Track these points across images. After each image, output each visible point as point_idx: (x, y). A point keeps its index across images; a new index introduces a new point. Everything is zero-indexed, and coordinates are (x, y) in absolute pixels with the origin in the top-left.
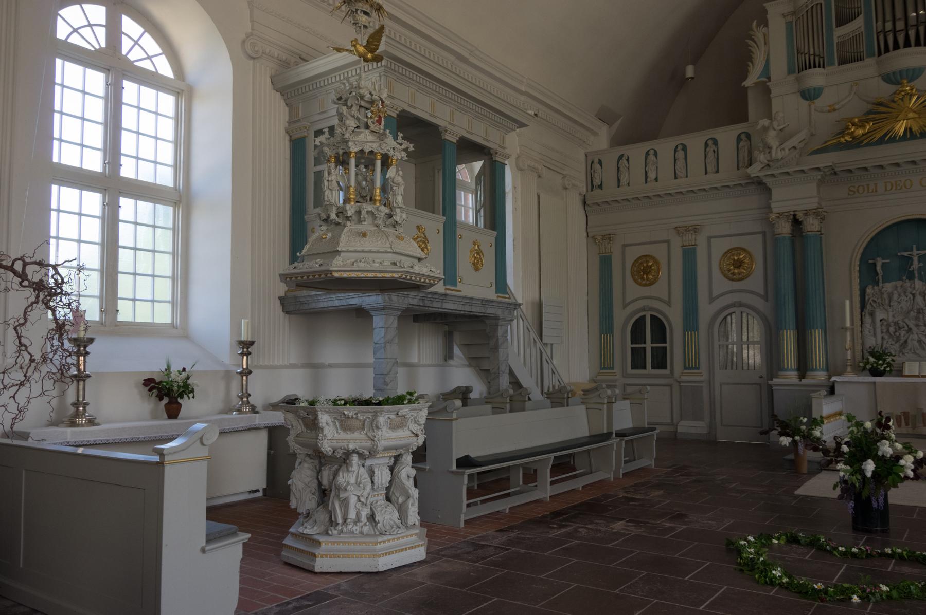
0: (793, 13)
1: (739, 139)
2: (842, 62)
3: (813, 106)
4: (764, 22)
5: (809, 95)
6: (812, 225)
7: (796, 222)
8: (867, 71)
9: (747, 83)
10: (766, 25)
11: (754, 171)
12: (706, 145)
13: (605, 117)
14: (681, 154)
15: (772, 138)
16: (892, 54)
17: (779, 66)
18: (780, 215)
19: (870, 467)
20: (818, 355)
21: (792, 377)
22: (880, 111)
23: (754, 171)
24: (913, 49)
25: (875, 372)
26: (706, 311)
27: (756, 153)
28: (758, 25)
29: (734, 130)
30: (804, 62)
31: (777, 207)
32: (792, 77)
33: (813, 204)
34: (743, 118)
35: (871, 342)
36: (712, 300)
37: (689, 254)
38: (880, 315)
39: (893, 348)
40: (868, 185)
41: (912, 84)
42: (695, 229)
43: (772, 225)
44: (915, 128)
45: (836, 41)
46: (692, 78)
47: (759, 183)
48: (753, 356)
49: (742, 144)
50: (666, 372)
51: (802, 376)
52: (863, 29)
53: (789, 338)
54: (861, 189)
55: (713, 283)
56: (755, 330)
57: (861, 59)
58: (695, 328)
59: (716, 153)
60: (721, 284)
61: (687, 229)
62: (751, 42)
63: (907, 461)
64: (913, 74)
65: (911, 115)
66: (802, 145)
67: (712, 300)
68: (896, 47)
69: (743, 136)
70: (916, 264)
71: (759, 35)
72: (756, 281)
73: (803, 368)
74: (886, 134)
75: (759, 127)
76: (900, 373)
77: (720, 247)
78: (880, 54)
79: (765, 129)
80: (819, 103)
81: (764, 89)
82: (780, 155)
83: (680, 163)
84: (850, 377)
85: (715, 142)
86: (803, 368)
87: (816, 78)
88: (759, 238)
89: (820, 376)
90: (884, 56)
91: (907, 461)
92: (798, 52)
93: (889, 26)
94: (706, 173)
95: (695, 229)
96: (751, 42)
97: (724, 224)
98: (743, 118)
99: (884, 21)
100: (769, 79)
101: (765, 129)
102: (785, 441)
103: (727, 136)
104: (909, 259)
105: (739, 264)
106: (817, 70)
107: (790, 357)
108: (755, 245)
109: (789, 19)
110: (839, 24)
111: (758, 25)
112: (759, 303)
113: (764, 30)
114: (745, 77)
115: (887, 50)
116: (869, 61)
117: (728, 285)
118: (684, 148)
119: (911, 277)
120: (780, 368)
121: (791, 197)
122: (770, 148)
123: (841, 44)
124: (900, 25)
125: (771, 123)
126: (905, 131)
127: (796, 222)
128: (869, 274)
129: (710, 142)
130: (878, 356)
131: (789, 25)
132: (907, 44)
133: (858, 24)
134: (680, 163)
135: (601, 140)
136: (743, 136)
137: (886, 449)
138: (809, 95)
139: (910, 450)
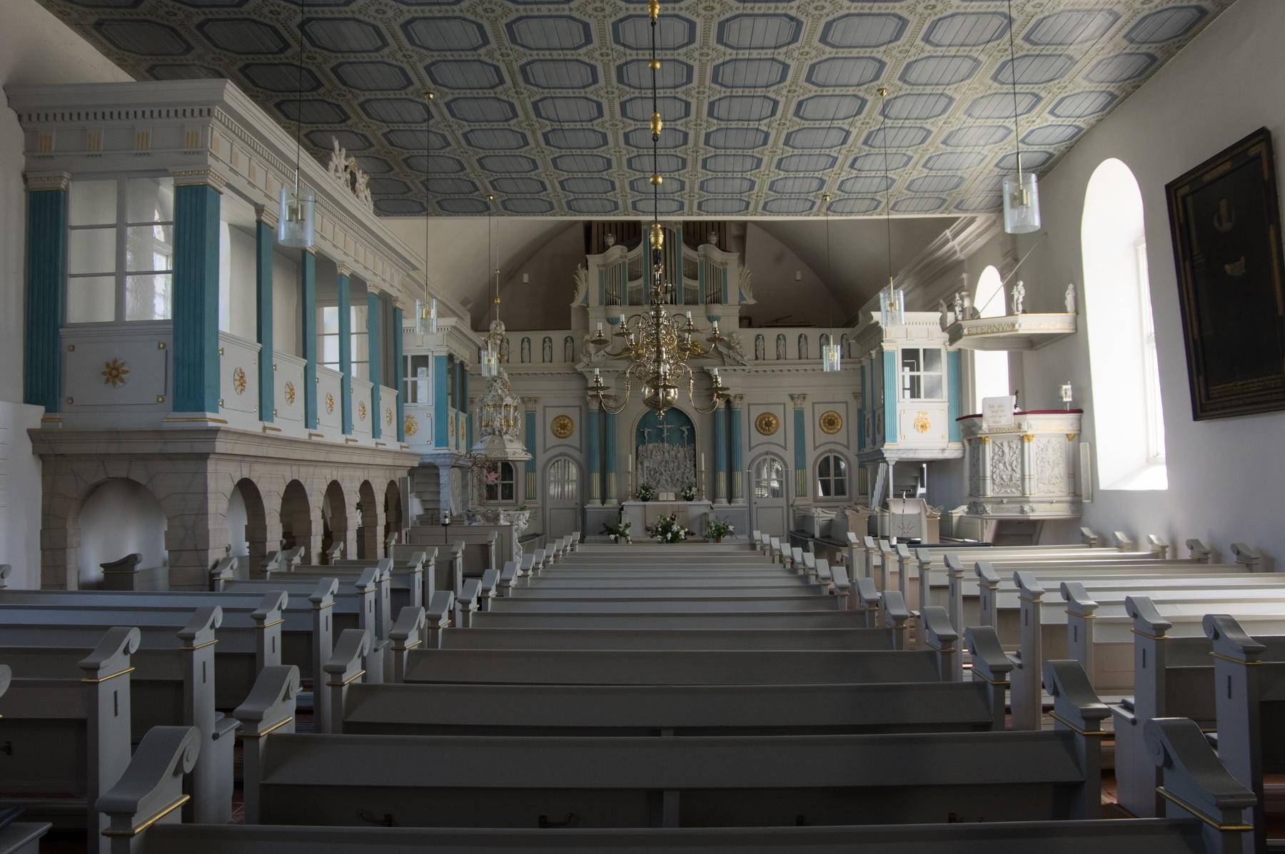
0: (604, 266)
2: (632, 304)
9: (574, 305)
11: (579, 367)
13: (464, 303)
14: (526, 345)
17: (594, 299)
19: (669, 535)
20: (613, 490)
21: (597, 503)
25: (645, 499)
30: (610, 302)
32: (602, 308)
35: (641, 481)
36: (545, 451)
38: (646, 464)
39: (653, 484)
42: (536, 401)
43: (587, 404)
48: (571, 488)
50: (512, 501)
51: (603, 503)
53: (596, 478)
55: (546, 436)
56: (574, 471)
58: (534, 471)
59: (551, 347)
60: (552, 440)
61: (530, 400)
63: (682, 533)
67: (545, 451)
70: (665, 434)
71: (582, 272)
72: (574, 439)
73: (604, 498)
76: (657, 499)
77: (552, 414)
81: (584, 310)
83: (526, 352)
84: (631, 502)
85: (550, 340)
86: (604, 498)
88: (577, 410)
89: (613, 502)
91: (682, 533)
95: (536, 401)
98: (569, 329)
103: (558, 337)
104: (662, 430)
105: (564, 427)
107: (597, 492)
108: (574, 414)
112: (576, 454)
119: (663, 441)
128: (641, 438)
131: (601, 272)
133: (640, 282)
139: (682, 528)
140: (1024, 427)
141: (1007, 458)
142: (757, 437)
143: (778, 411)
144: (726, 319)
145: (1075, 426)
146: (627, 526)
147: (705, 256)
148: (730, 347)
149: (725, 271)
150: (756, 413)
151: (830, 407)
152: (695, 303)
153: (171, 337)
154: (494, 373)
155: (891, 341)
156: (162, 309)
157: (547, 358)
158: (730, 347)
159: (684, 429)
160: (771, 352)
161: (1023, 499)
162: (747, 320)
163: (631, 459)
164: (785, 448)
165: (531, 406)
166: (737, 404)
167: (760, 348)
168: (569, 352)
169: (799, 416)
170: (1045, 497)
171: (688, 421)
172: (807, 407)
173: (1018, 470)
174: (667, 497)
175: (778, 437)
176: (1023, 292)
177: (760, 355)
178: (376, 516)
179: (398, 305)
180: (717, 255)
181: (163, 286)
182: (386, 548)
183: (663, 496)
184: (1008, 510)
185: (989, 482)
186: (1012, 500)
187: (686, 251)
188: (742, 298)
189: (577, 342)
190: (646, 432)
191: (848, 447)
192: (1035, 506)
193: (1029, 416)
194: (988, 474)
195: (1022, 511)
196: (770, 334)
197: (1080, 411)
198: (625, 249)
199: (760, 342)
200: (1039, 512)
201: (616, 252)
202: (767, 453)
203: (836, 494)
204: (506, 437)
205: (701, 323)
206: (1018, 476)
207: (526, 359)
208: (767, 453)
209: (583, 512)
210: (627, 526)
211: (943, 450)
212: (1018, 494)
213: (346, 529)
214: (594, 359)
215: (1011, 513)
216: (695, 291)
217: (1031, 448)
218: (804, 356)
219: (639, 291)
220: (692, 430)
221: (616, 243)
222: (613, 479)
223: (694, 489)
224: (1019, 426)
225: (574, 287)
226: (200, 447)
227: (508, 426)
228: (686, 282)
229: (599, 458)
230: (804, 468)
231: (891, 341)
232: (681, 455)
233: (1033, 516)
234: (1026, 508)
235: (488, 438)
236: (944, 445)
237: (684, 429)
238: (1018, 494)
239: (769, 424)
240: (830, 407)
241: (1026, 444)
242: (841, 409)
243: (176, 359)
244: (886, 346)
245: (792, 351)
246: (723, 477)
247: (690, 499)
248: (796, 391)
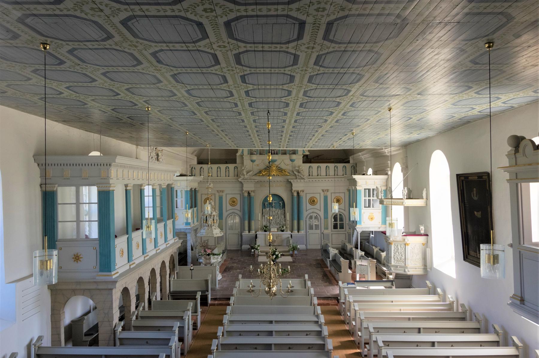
2: (260, 154)
5: (253, 161)
6: (252, 194)
7: (249, 193)
9: (238, 154)
11: (240, 180)
14: (219, 169)
18: (245, 191)
19: (275, 256)
20: (253, 227)
22: (268, 168)
23: (240, 180)
24: (275, 155)
25: (265, 231)
26: (225, 214)
29: (234, 165)
31: (245, 189)
33: (253, 189)
34: (236, 163)
35: (264, 224)
36: (227, 211)
37: (221, 198)
38: (266, 216)
39: (268, 225)
42: (223, 191)
43: (243, 193)
47: (241, 182)
51: (249, 232)
56: (237, 220)
61: (221, 191)
63: (279, 255)
67: (227, 211)
72: (238, 207)
77: (229, 197)
80: (255, 163)
83: (219, 172)
87: (254, 157)
89: (253, 232)
91: (279, 255)
95: (223, 191)
97: (230, 191)
98: (236, 163)
102: (253, 250)
103: (231, 166)
105: (234, 202)
108: (238, 197)
117: (231, 207)
118: (220, 168)
119: (272, 207)
120: (244, 230)
121: (248, 187)
127: (249, 193)
128: (264, 206)
130: (266, 227)
134: (219, 172)
135: (195, 161)
137: (277, 253)
138: (253, 161)
140: (406, 241)
141: (399, 251)
142: (309, 206)
143: (317, 196)
145: (426, 241)
146: (258, 246)
148: (299, 172)
150: (309, 196)
151: (338, 195)
153: (98, 245)
154: (210, 213)
155: (360, 186)
156: (95, 234)
157: (227, 175)
158: (299, 172)
159: (281, 203)
160: (315, 173)
161: (405, 267)
163: (260, 215)
164: (320, 210)
165: (221, 194)
166: (301, 194)
167: (311, 171)
169: (326, 198)
170: (413, 267)
171: (282, 200)
172: (329, 194)
173: (404, 256)
174: (274, 230)
175: (317, 206)
176: (407, 191)
177: (311, 174)
178: (166, 272)
179: (173, 186)
181: (95, 227)
182: (170, 282)
183: (272, 230)
184: (400, 270)
185: (393, 259)
186: (401, 267)
189: (239, 169)
190: (265, 204)
191: (345, 210)
192: (409, 270)
193: (408, 237)
194: (392, 256)
195: (405, 271)
196: (315, 166)
197: (427, 235)
200: (410, 272)
202: (313, 213)
203: (340, 228)
204: (213, 227)
205: (288, 161)
206: (404, 258)
207: (219, 175)
208: (313, 213)
209: (241, 236)
210: (258, 246)
211: (379, 228)
212: (403, 265)
213: (156, 283)
214: (246, 176)
215: (401, 272)
217: (408, 248)
218: (328, 174)
220: (284, 203)
222: (253, 223)
223: (284, 227)
224: (404, 240)
226: (110, 287)
227: (214, 222)
229: (248, 215)
230: (327, 218)
231: (360, 186)
232: (279, 213)
233: (409, 273)
234: (406, 270)
235: (206, 228)
236: (380, 226)
237: (281, 203)
238: (403, 265)
239: (314, 201)
240: (338, 195)
241: (407, 247)
242: (342, 195)
243: (100, 254)
244: (358, 188)
245: (323, 173)
246: (296, 222)
247: (283, 231)
248: (326, 188)
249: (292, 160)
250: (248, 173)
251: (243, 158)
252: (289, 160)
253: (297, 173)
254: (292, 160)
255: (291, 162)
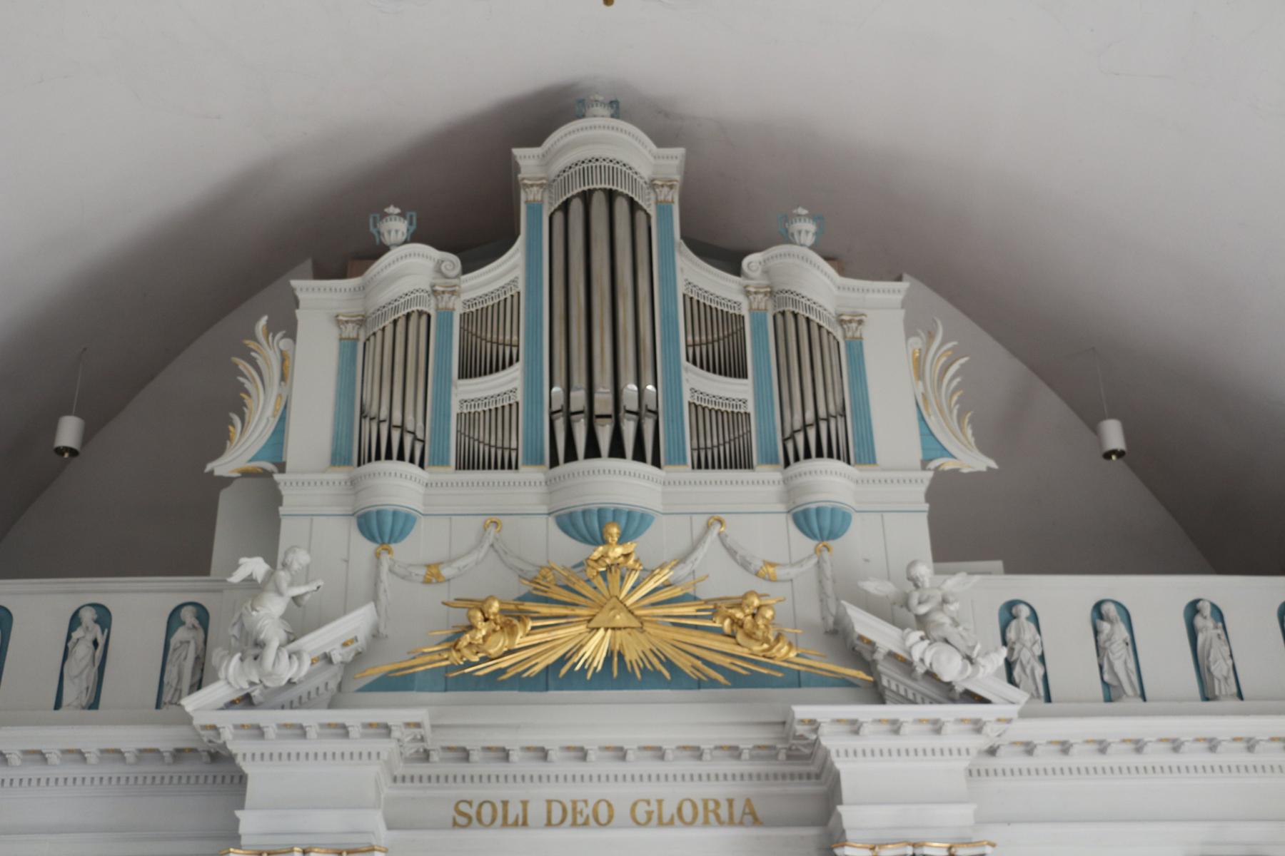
0: (362, 322)
1: (174, 620)
2: (467, 462)
3: (385, 559)
4: (287, 325)
5: (379, 527)
8: (525, 488)
9: (223, 467)
10: (292, 334)
12: (75, 621)
15: (269, 615)
16: (583, 464)
24: (628, 464)
27: (215, 655)
28: (271, 329)
32: (340, 475)
40: (505, 803)
41: (630, 547)
44: (631, 656)
45: (455, 409)
46: (73, 452)
49: (180, 634)
52: (519, 397)
54: (487, 810)
57: (511, 465)
59: (102, 650)
62: (243, 365)
64: (633, 523)
65: (621, 619)
66: (348, 654)
68: (593, 450)
69: (188, 615)
71: (268, 352)
74: (562, 660)
75: (236, 578)
78: (554, 462)
79: (253, 588)
80: (403, 551)
81: (264, 484)
82: (287, 670)
85: (104, 617)
87: (399, 484)
90: (564, 468)
92: (363, 415)
93: (579, 399)
94: (58, 706)
96: (243, 365)
99: (568, 389)
100: (282, 468)
101: (253, 588)
106: (405, 466)
109: (350, 331)
110: (467, 371)
111: (271, 329)
113: (284, 344)
114: (218, 450)
115: (571, 455)
116: (532, 475)
122: (260, 645)
123: (468, 420)
124: (603, 402)
125: (270, 575)
126: (608, 659)
129: (88, 616)
131: (348, 346)
132: (617, 450)
133: (508, 382)
136: (188, 615)
138: (379, 527)
144: (882, 505)
147: (771, 294)
149: (856, 348)
152: (741, 461)
162: (965, 527)
168: (197, 677)
180: (822, 288)
187: (695, 275)
188: (932, 447)
198: (452, 261)
199: (1022, 630)
201: (411, 269)
216: (737, 419)
219: (502, 414)
221: (414, 238)
225: (235, 403)
228: (700, 384)
249: (817, 524)
250: (300, 621)
251: (277, 499)
252: (783, 526)
253: (884, 636)
254: (817, 524)
255: (804, 545)
